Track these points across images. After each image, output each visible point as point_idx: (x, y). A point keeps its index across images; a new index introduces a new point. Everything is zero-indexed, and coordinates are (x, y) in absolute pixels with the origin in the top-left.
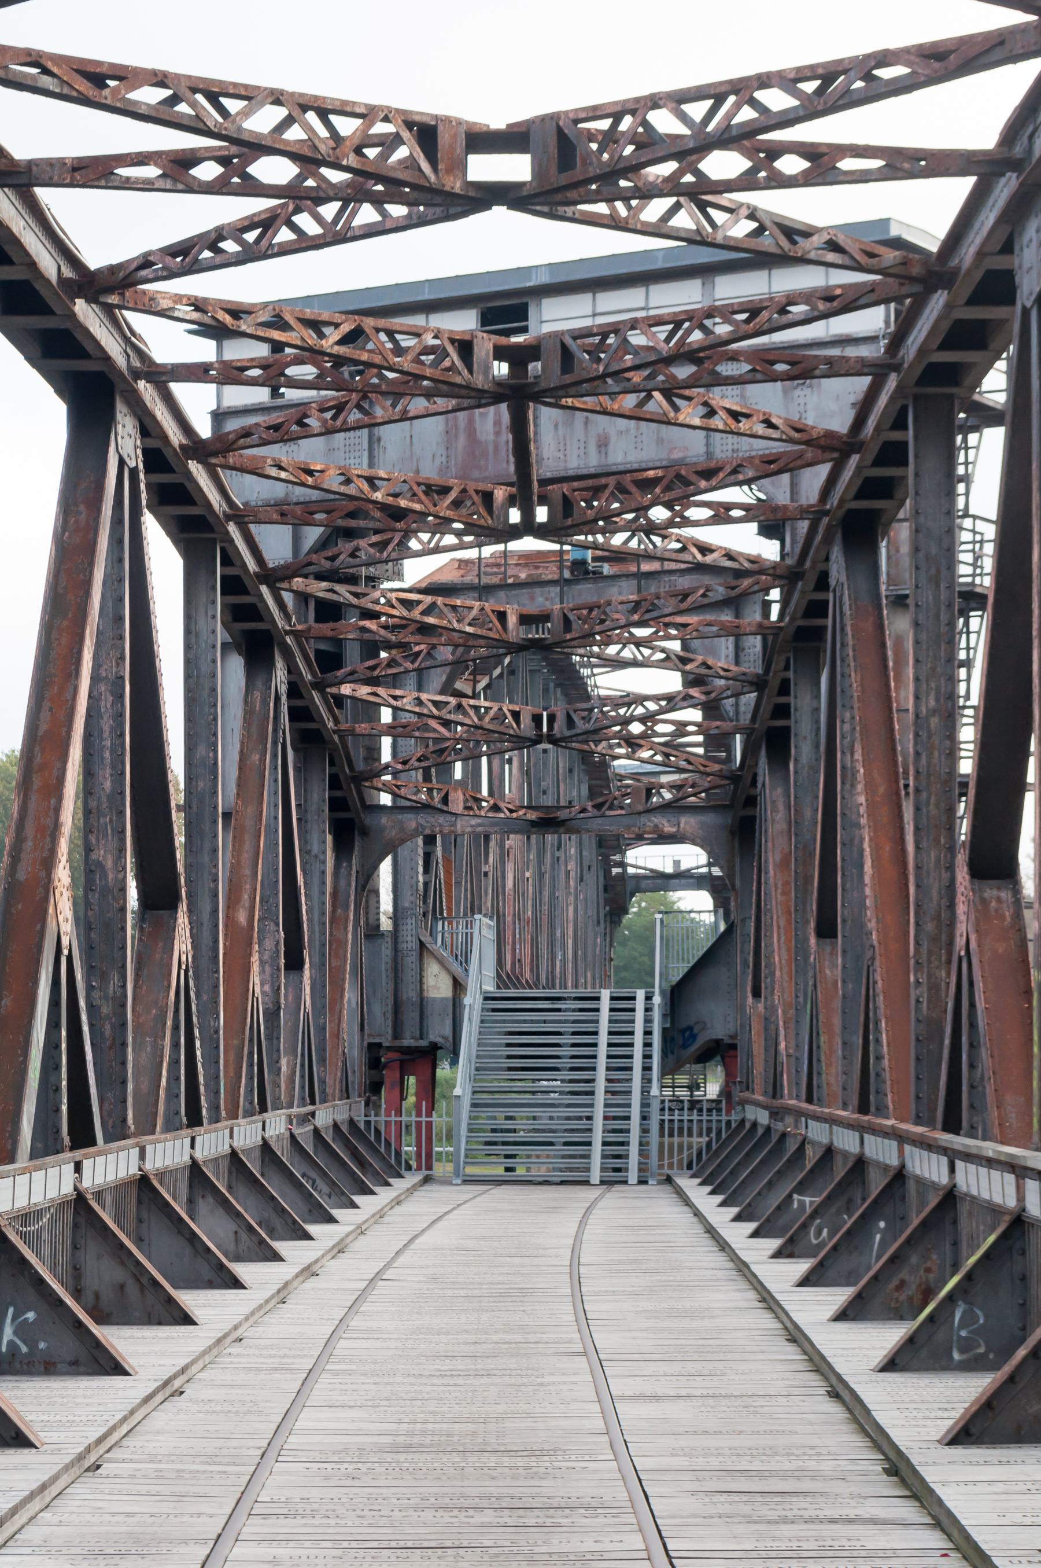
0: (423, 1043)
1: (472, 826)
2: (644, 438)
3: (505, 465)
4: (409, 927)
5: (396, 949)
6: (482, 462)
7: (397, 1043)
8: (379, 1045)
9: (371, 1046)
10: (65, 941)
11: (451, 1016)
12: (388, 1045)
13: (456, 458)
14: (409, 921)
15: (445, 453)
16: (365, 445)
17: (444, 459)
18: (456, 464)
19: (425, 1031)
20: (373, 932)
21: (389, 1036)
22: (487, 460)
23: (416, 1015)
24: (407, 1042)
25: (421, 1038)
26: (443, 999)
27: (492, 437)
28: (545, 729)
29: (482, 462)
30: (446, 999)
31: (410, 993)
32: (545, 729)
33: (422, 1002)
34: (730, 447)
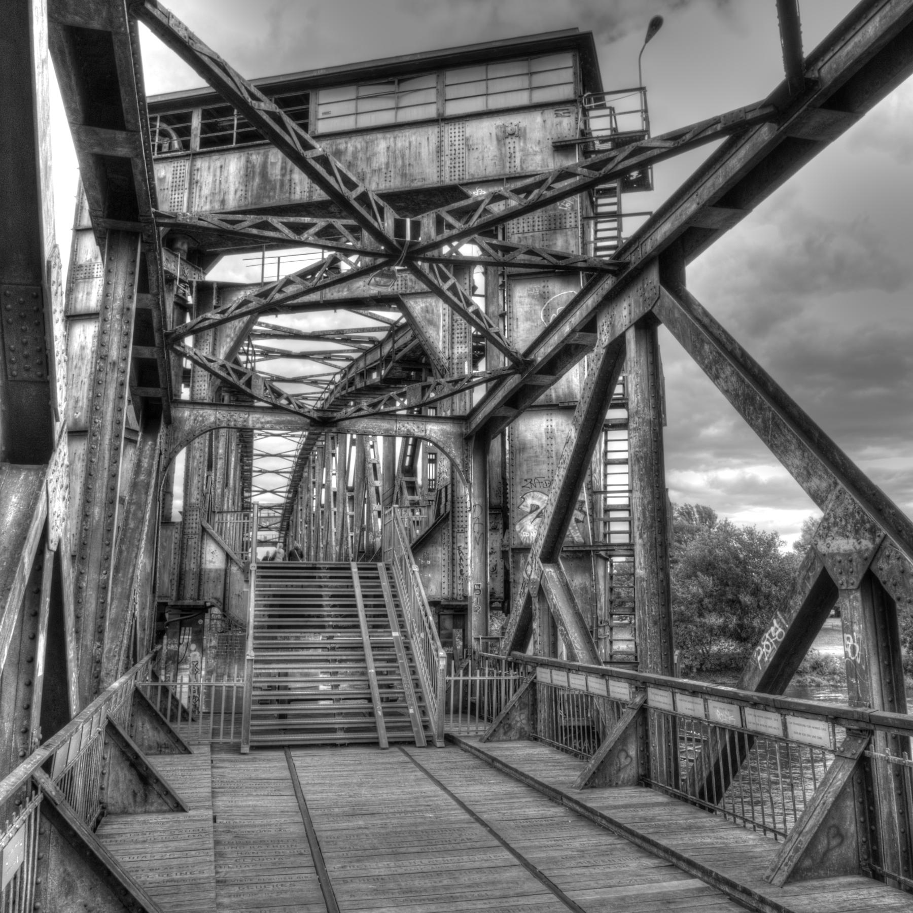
0: (201, 603)
1: (262, 423)
2: (392, 174)
3: (287, 195)
4: (195, 517)
5: (183, 533)
6: (271, 194)
7: (180, 603)
8: (165, 604)
9: (159, 604)
10: (54, 535)
11: (223, 582)
12: (172, 603)
13: (252, 191)
14: (195, 513)
15: (244, 188)
16: (187, 186)
17: (243, 193)
18: (252, 196)
19: (202, 593)
20: (166, 521)
21: (174, 597)
22: (275, 192)
23: (195, 582)
24: (188, 602)
25: (199, 599)
26: (216, 570)
27: (279, 177)
28: (408, 237)
29: (271, 194)
30: (220, 570)
31: (192, 566)
32: (408, 237)
33: (200, 574)
34: (457, 177)
